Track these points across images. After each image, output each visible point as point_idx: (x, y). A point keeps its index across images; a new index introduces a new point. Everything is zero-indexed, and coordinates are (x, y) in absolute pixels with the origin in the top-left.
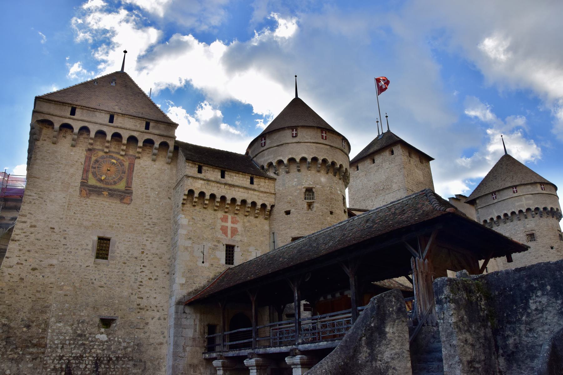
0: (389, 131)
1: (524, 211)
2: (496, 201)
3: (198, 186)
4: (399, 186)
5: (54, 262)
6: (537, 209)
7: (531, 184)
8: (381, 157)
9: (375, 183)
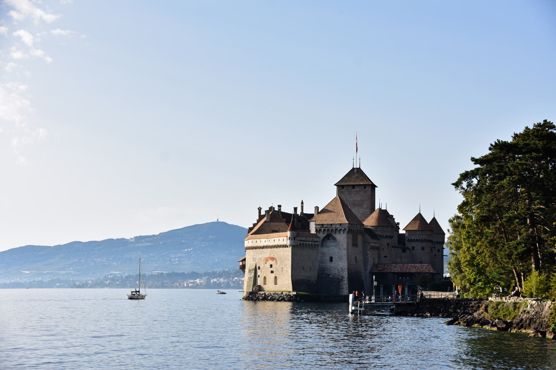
0: (360, 168)
1: (423, 239)
2: (414, 233)
3: (372, 244)
4: (367, 206)
5: (351, 263)
6: (427, 239)
7: (427, 231)
8: (359, 188)
9: (353, 200)
